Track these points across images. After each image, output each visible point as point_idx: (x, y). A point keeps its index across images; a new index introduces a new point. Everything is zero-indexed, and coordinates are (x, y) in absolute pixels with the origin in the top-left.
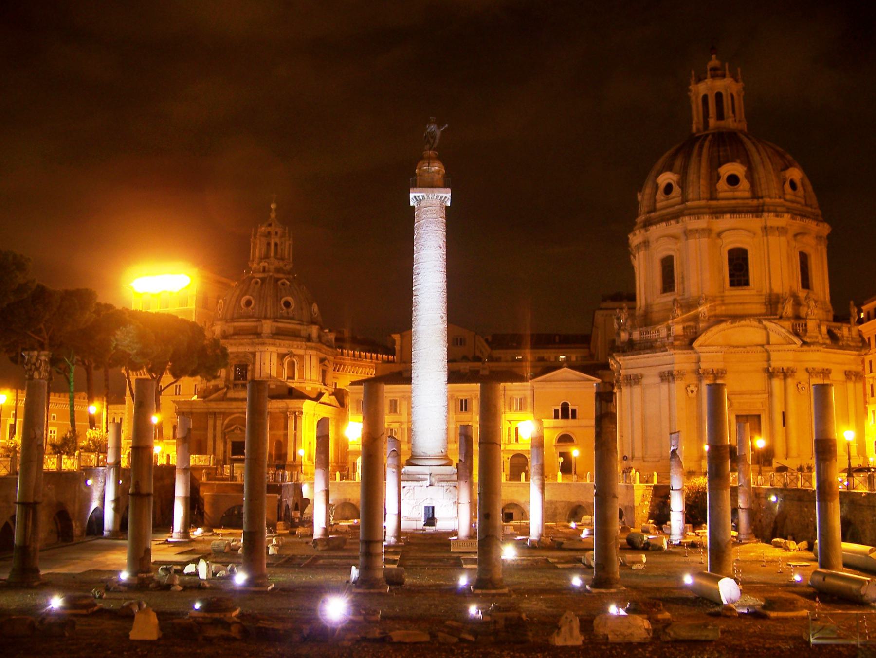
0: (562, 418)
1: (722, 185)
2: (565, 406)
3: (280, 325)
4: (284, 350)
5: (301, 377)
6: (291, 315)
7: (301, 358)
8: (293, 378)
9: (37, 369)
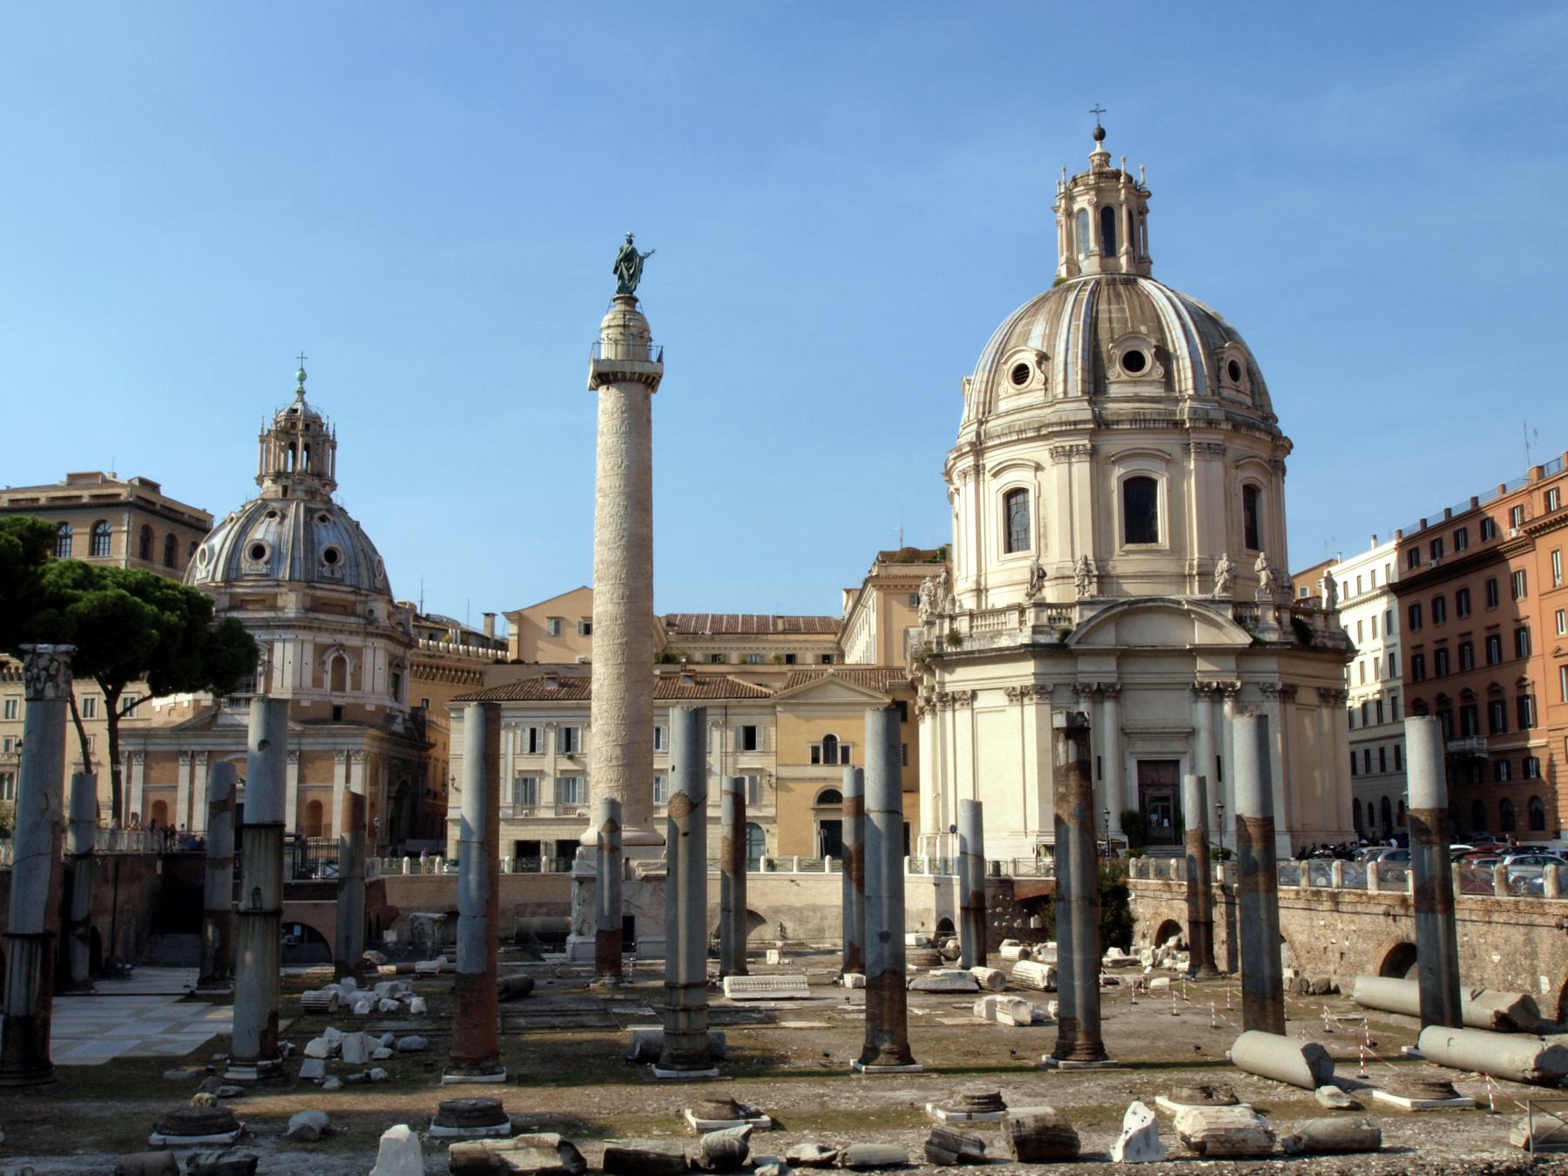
0: (827, 761)
1: (1116, 371)
2: (830, 740)
3: (318, 593)
4: (326, 639)
5: (357, 685)
6: (338, 575)
7: (358, 652)
8: (342, 689)
9: (51, 678)
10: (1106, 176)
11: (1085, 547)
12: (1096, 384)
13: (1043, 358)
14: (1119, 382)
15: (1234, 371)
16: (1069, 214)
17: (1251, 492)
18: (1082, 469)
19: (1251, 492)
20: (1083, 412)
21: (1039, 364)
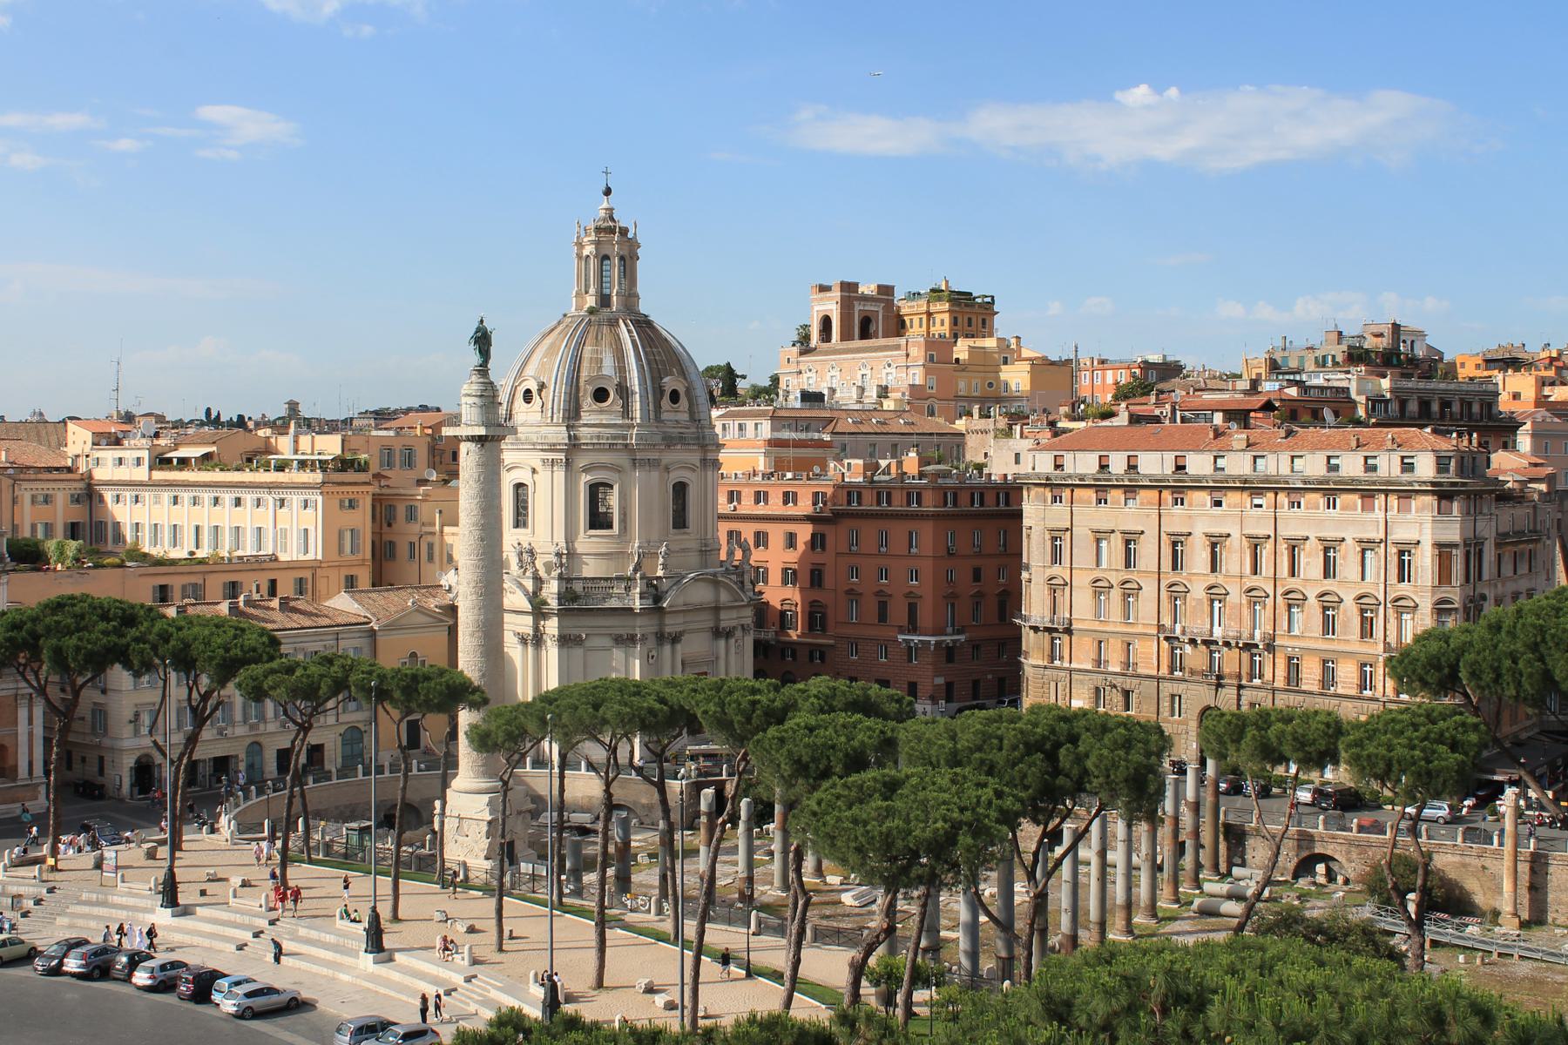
1: (587, 402)
10: (608, 229)
11: (560, 537)
12: (572, 413)
13: (542, 387)
14: (590, 413)
15: (675, 397)
16: (579, 256)
17: (680, 489)
18: (560, 475)
19: (680, 489)
20: (559, 434)
21: (540, 391)
